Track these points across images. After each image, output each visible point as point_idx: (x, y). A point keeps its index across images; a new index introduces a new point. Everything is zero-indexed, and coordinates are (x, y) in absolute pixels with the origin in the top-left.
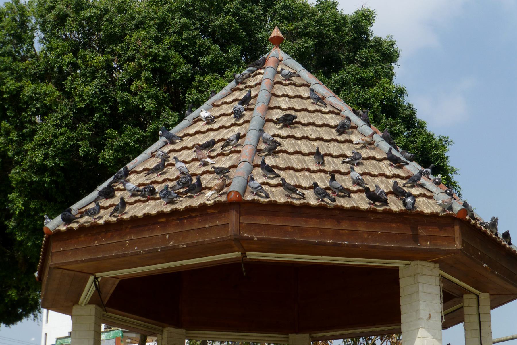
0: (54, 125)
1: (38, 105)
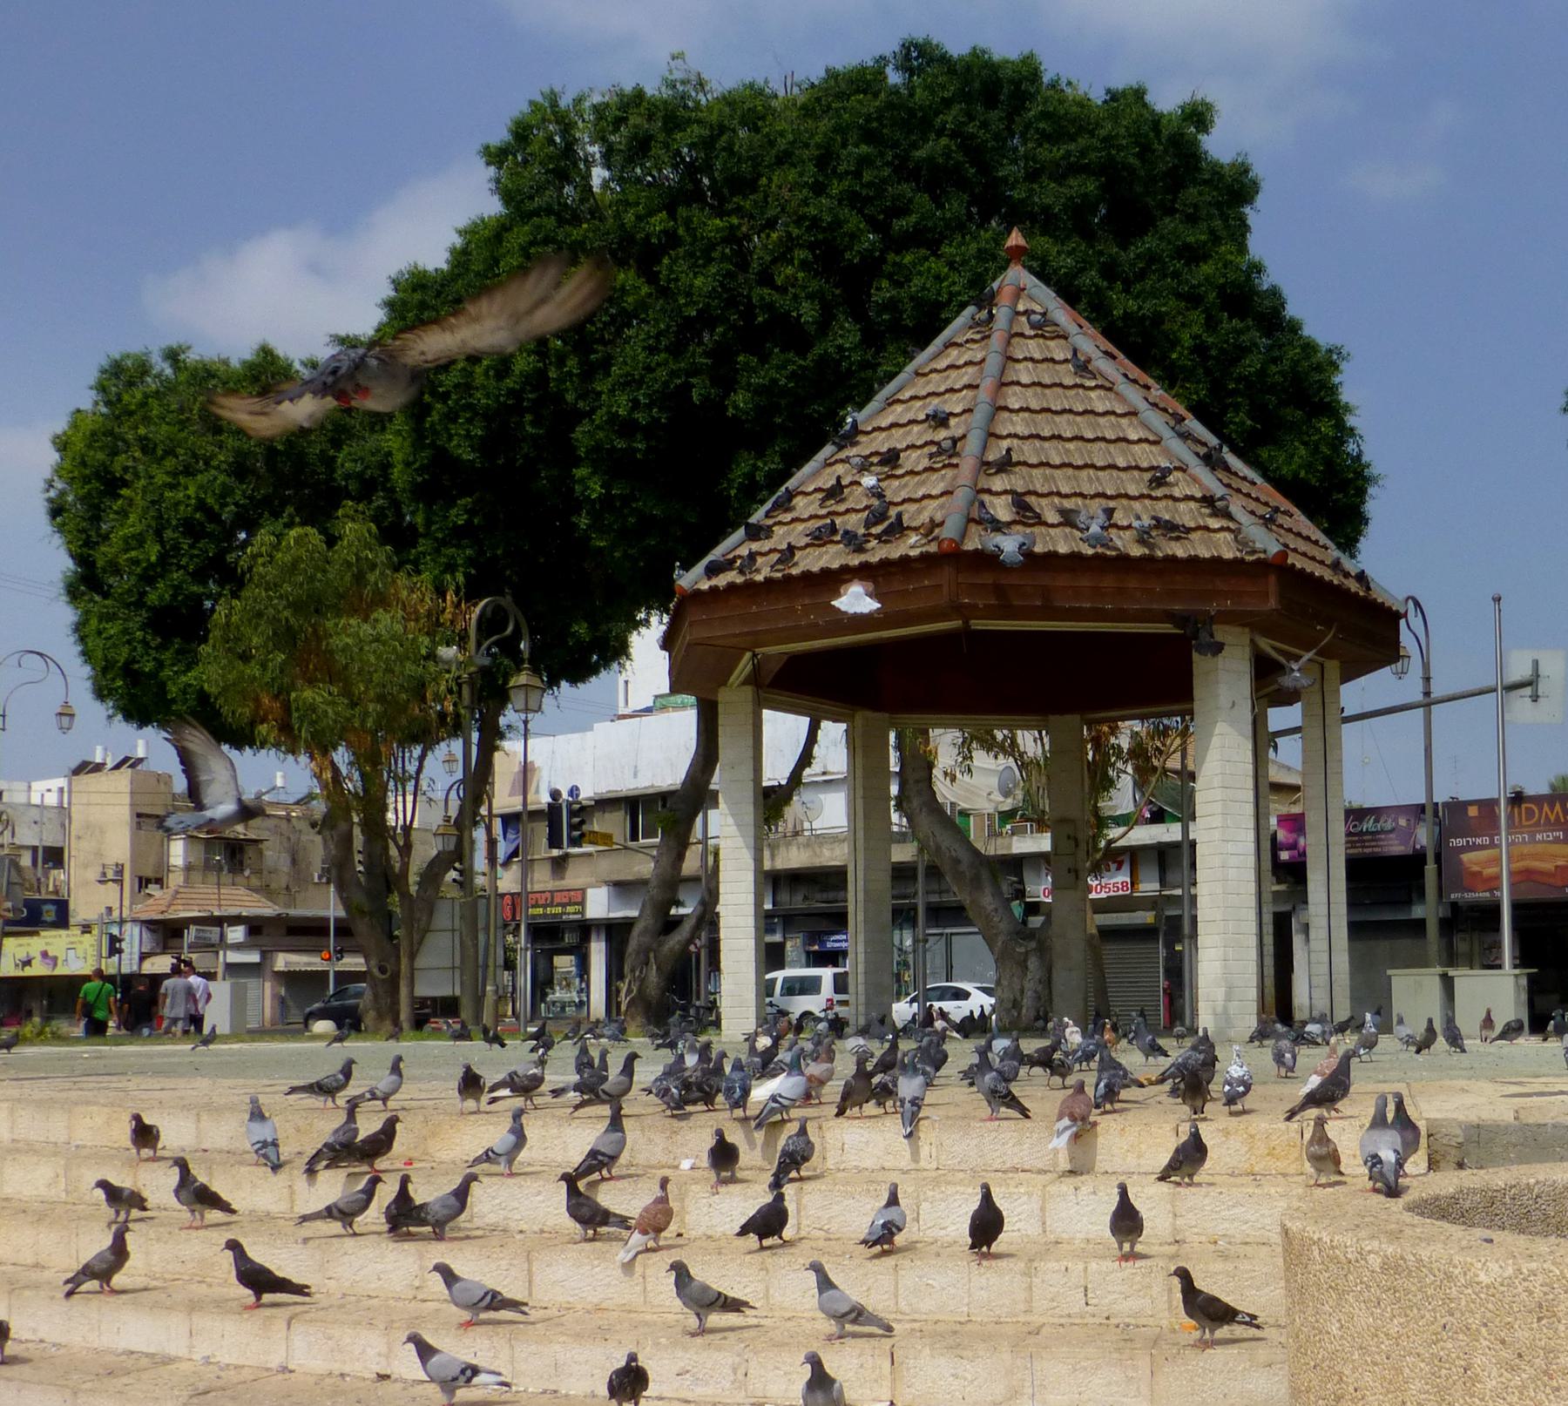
1: (613, 311)
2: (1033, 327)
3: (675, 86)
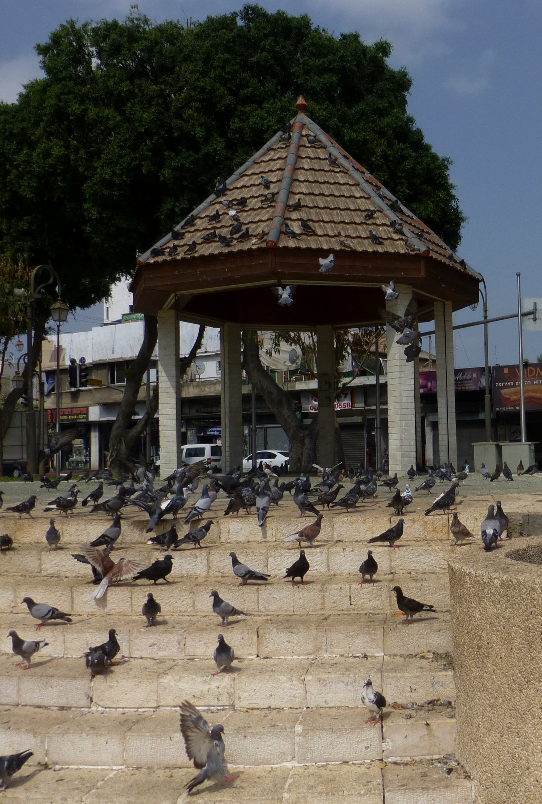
0: (118, 146)
2: (310, 142)
3: (133, 21)
